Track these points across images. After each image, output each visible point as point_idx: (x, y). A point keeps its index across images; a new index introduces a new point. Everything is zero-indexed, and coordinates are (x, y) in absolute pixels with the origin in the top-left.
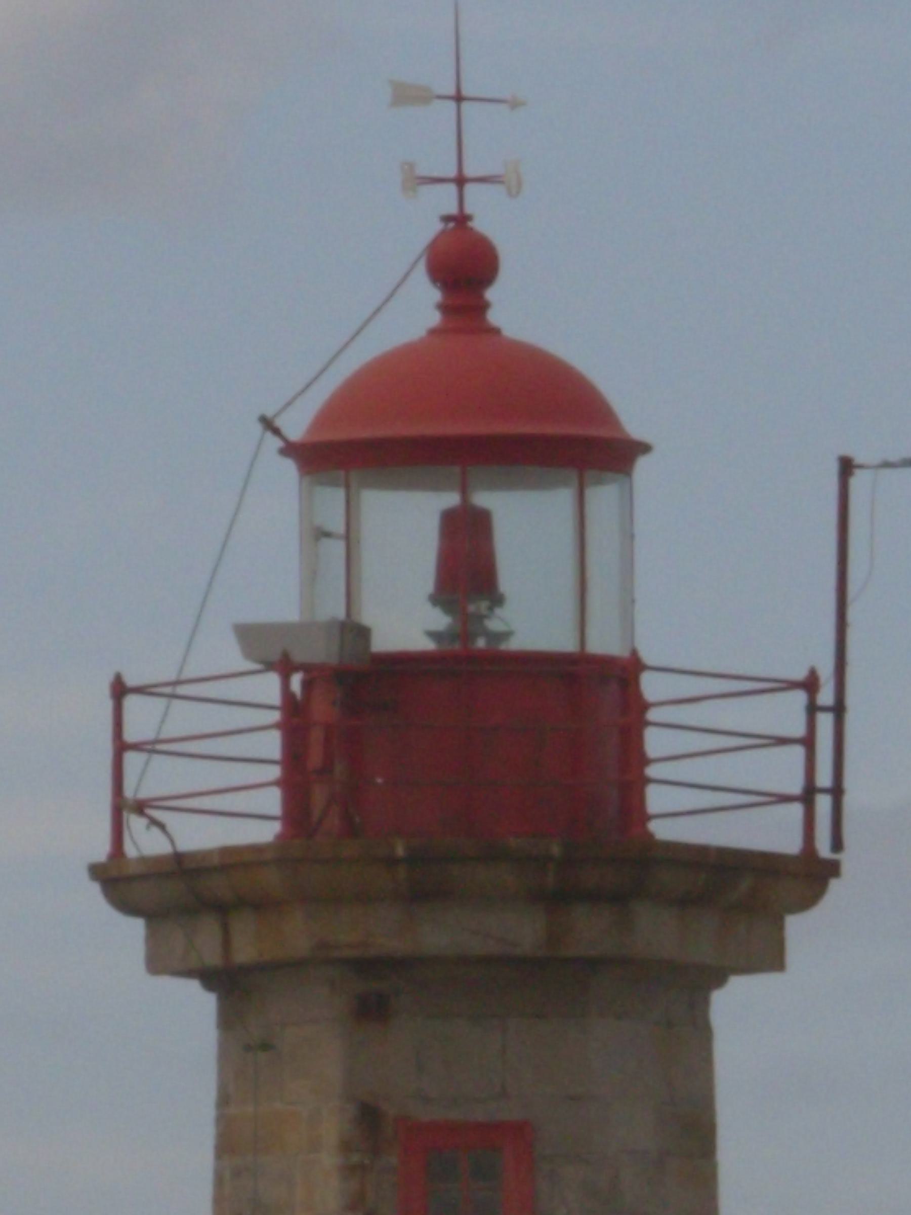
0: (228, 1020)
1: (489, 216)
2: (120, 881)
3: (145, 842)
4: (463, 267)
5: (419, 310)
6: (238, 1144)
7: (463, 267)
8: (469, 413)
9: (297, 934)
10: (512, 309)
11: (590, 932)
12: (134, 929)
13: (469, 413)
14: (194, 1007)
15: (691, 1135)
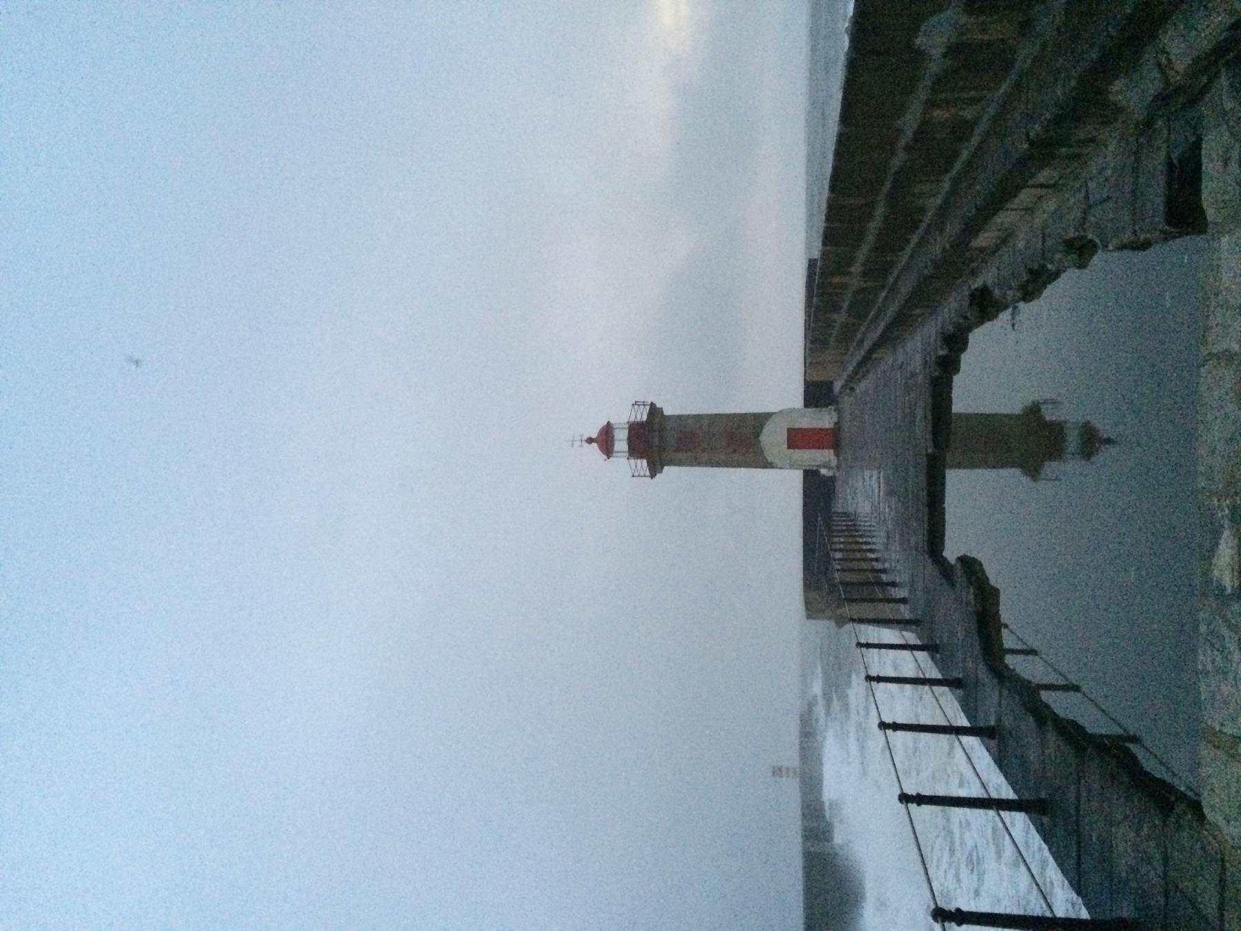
0: (668, 464)
1: (585, 438)
2: (652, 476)
3: (648, 473)
4: (590, 440)
5: (595, 445)
6: (679, 463)
7: (590, 440)
8: (605, 440)
9: (657, 458)
10: (594, 436)
11: (656, 426)
12: (658, 475)
13: (605, 440)
14: (666, 468)
15: (679, 417)
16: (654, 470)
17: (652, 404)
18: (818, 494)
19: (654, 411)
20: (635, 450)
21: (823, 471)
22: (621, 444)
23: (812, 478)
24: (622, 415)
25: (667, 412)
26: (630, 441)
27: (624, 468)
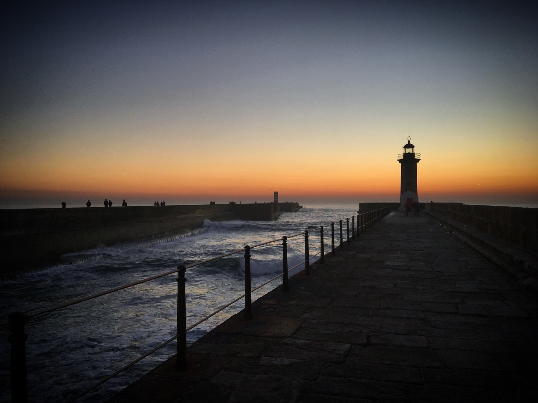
4: (409, 141)
7: (409, 141)
8: (409, 146)
13: (409, 146)
16: (400, 161)
17: (420, 160)
18: (393, 207)
19: (418, 160)
20: (405, 155)
21: (400, 208)
22: (408, 151)
23: (398, 205)
24: (417, 151)
25: (417, 164)
26: (409, 153)
27: (400, 152)
